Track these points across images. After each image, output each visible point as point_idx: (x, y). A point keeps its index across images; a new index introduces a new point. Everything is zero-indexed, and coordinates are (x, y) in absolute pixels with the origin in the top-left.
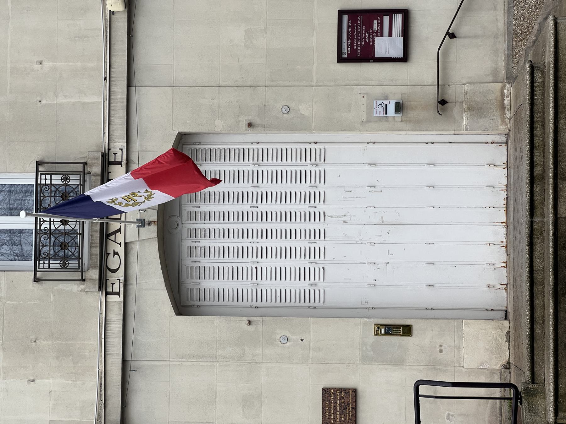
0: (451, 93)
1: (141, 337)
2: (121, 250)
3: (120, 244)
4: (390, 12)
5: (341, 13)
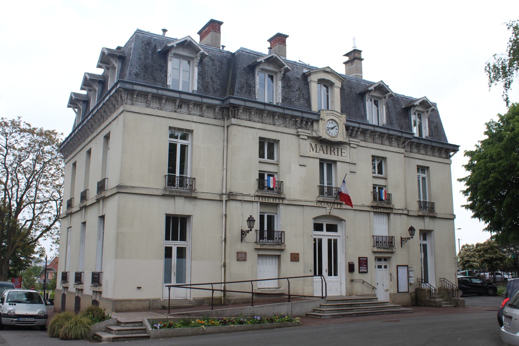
1: (306, 209)
2: (325, 206)
4: (367, 269)
5: (367, 258)
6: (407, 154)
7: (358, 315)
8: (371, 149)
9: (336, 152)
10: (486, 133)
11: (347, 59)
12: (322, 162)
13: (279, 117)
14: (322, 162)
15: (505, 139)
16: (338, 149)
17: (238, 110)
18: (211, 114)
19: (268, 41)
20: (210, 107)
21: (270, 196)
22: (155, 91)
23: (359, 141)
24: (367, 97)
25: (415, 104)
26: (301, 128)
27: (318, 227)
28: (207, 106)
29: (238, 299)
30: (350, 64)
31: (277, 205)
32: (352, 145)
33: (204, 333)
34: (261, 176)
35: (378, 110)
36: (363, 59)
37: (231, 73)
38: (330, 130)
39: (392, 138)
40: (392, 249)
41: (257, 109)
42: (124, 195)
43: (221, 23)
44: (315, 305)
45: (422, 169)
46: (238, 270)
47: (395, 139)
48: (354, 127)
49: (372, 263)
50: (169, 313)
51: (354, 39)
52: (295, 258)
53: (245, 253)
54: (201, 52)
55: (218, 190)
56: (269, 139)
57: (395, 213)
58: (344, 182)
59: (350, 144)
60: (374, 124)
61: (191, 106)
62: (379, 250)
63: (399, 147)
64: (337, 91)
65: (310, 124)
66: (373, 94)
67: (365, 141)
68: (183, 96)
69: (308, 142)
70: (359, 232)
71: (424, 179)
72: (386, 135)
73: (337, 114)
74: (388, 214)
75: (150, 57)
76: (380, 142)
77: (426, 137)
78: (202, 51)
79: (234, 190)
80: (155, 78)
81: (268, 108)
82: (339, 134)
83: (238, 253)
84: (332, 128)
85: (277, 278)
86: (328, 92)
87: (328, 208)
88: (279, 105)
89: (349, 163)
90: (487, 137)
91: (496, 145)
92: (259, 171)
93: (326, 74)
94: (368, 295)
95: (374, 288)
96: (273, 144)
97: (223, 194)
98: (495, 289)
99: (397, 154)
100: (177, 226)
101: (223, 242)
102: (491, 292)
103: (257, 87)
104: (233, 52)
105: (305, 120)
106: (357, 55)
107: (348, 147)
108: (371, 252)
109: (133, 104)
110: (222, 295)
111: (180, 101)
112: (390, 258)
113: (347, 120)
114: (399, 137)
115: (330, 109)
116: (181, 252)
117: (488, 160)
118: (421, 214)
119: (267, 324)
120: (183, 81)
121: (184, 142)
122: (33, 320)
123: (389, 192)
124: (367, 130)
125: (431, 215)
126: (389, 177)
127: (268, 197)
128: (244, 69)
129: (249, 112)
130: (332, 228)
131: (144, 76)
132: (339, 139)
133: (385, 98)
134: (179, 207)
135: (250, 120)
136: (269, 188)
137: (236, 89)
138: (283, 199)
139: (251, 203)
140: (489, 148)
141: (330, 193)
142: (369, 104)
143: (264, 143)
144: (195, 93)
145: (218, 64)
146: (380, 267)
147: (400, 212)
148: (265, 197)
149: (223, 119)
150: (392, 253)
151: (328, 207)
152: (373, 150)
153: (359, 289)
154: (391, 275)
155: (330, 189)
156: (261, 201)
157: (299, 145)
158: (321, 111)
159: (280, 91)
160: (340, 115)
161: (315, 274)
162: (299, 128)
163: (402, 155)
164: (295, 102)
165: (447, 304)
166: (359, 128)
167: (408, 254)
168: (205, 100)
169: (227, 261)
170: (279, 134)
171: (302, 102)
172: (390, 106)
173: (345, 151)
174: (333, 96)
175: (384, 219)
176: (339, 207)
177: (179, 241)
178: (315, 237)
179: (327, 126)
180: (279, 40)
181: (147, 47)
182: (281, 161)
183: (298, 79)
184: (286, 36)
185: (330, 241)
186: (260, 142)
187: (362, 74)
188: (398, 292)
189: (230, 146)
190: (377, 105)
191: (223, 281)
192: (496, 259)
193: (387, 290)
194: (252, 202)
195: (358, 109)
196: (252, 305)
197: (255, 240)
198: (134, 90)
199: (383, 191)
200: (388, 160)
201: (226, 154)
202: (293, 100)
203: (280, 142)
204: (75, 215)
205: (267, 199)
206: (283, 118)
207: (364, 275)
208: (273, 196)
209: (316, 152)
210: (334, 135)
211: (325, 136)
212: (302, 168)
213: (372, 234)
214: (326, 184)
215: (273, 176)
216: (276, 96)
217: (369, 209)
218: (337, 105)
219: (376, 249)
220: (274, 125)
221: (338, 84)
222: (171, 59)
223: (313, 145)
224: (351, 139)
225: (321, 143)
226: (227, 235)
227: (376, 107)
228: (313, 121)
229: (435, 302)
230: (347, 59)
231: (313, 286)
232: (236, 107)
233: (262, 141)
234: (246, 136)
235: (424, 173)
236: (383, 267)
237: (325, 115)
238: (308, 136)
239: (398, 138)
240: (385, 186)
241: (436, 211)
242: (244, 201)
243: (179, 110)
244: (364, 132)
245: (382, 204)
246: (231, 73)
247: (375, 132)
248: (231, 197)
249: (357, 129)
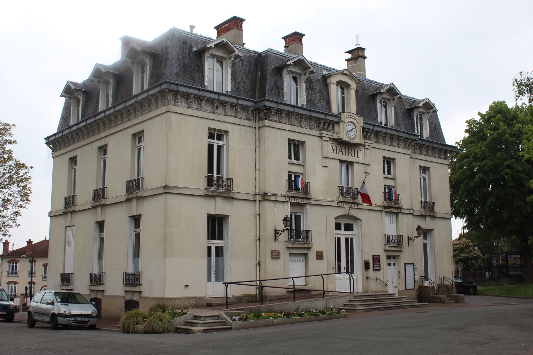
0: (369, 280)
1: (329, 209)
4: (380, 266)
6: (412, 155)
7: (385, 309)
8: (383, 151)
10: (466, 131)
11: (349, 56)
15: (488, 140)
17: (271, 112)
18: (242, 114)
19: (283, 38)
20: (245, 108)
22: (196, 92)
25: (419, 105)
27: (338, 227)
28: (242, 107)
29: (273, 296)
30: (353, 61)
31: (303, 205)
32: (367, 147)
33: (273, 325)
36: (366, 58)
37: (259, 74)
40: (401, 248)
42: (171, 195)
43: (242, 20)
44: (345, 300)
45: (424, 169)
46: (273, 268)
48: (369, 129)
49: (384, 261)
50: (227, 308)
51: (357, 36)
52: (320, 256)
53: (279, 252)
54: (236, 53)
55: (251, 190)
57: (402, 213)
58: (364, 183)
61: (204, 102)
62: (390, 248)
64: (353, 93)
65: (331, 126)
66: (384, 96)
68: (222, 98)
70: (373, 231)
71: (424, 179)
72: (396, 137)
74: (397, 214)
75: (188, 57)
76: (389, 143)
77: (427, 138)
78: (237, 52)
79: (268, 190)
80: (193, 79)
81: (297, 111)
83: (272, 251)
84: (351, 131)
85: (304, 275)
87: (347, 208)
88: (304, 107)
90: (467, 135)
91: (480, 144)
93: (344, 76)
94: (381, 292)
95: (386, 285)
96: (298, 145)
97: (256, 194)
98: (475, 288)
99: (405, 155)
100: (216, 225)
101: (258, 241)
102: (471, 291)
103: (285, 89)
104: (260, 52)
105: (327, 122)
106: (360, 53)
107: (363, 148)
108: (383, 251)
109: (175, 105)
110: (258, 292)
111: (217, 102)
112: (398, 256)
113: (363, 123)
114: (406, 138)
116: (220, 251)
117: (471, 159)
118: (423, 213)
119: (321, 316)
120: (217, 81)
121: (220, 143)
122: (87, 319)
123: (398, 193)
124: (380, 132)
125: (432, 214)
127: (297, 197)
128: (273, 71)
130: (349, 227)
131: (184, 76)
132: (357, 141)
134: (220, 207)
137: (267, 91)
138: (309, 199)
140: (472, 147)
144: (229, 94)
145: (245, 63)
146: (389, 265)
147: (407, 212)
149: (255, 120)
150: (401, 251)
151: (347, 207)
152: (385, 151)
153: (374, 287)
154: (399, 272)
157: (322, 147)
159: (304, 93)
161: (339, 271)
162: (322, 130)
163: (408, 156)
164: (317, 104)
165: (447, 300)
166: (373, 130)
167: (412, 253)
168: (240, 102)
169: (261, 260)
174: (349, 98)
175: (393, 218)
177: (217, 241)
178: (347, 236)
179: (347, 128)
180: (294, 39)
181: (184, 46)
183: (319, 80)
184: (303, 35)
185: (347, 239)
186: (289, 143)
187: (365, 72)
188: (406, 289)
189: (262, 147)
191: (258, 279)
192: (472, 259)
193: (395, 287)
194: (283, 202)
195: (370, 110)
196: (294, 301)
197: (286, 239)
198: (179, 91)
201: (258, 155)
202: (315, 102)
203: (306, 144)
204: (79, 213)
205: (296, 199)
207: (377, 272)
210: (352, 137)
211: (346, 139)
212: (325, 169)
213: (384, 234)
216: (301, 98)
217: (381, 209)
218: (352, 106)
219: (387, 248)
221: (354, 86)
222: (207, 60)
223: (334, 147)
224: (366, 141)
226: (261, 234)
229: (439, 298)
230: (349, 56)
231: (335, 282)
232: (269, 109)
234: (277, 137)
235: (425, 174)
236: (392, 265)
238: (330, 138)
240: (394, 187)
241: (436, 211)
242: (277, 201)
243: (216, 111)
244: (377, 134)
245: (392, 204)
246: (259, 74)
247: (387, 134)
248: (265, 197)
249: (373, 132)
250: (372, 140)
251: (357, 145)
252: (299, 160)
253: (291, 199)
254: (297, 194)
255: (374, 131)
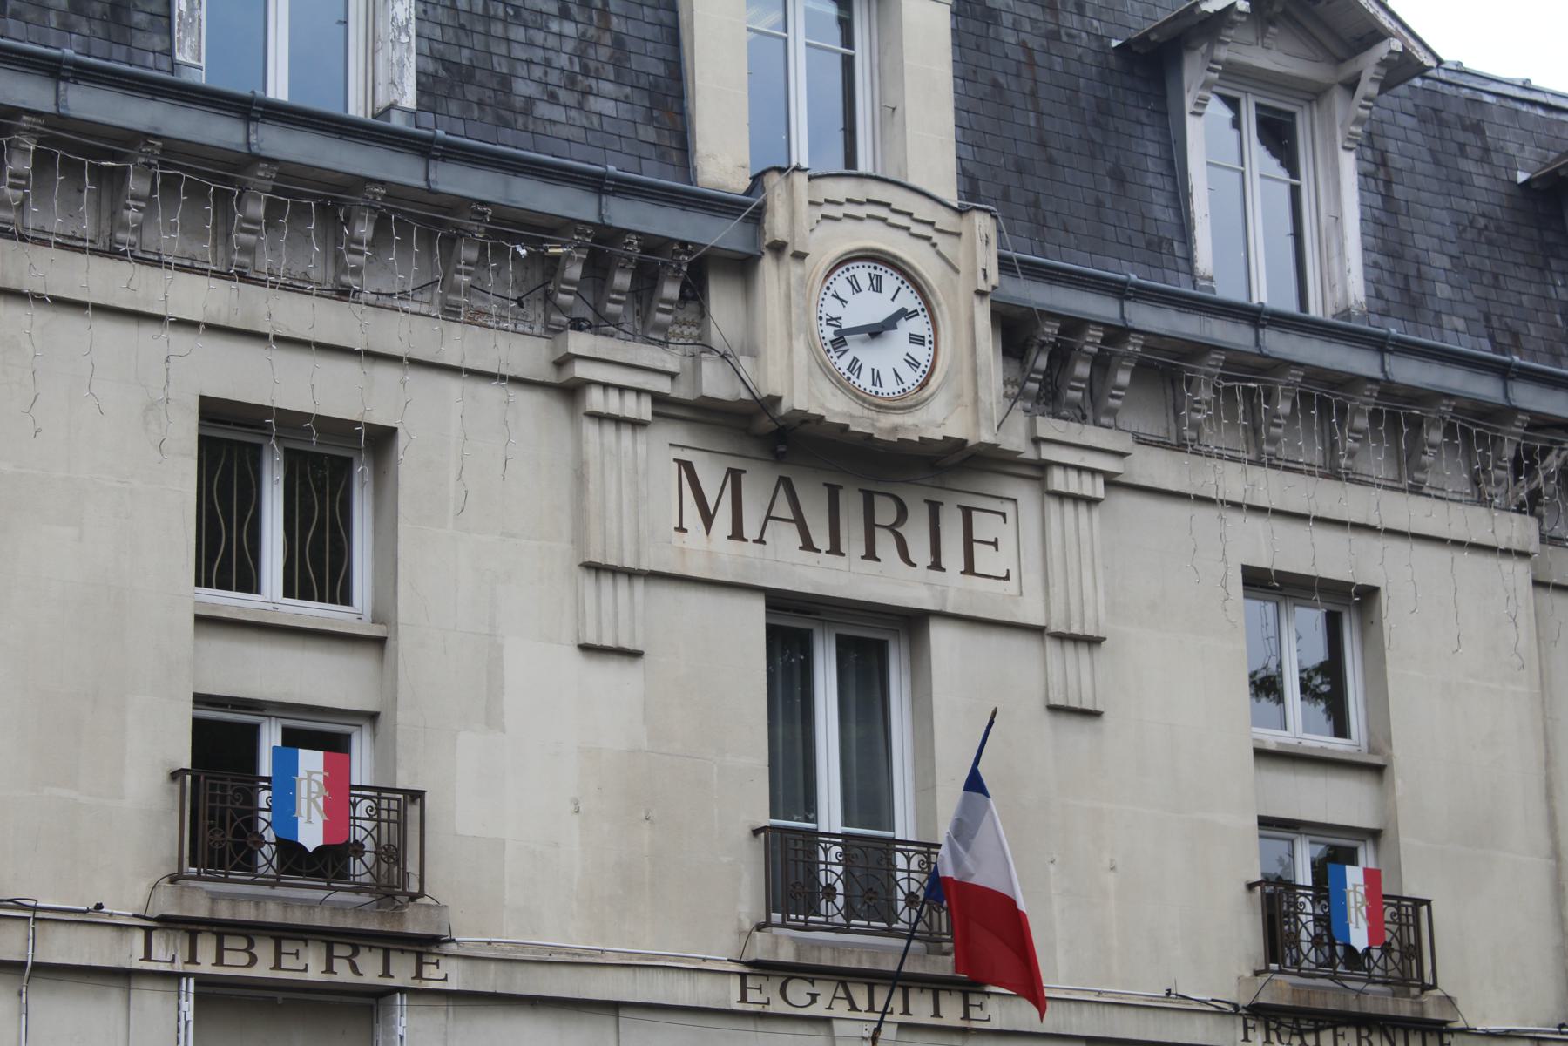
2: (818, 1010)
3: (830, 1008)
8: (1236, 519)
9: (917, 536)
12: (792, 623)
13: (381, 225)
14: (792, 623)
16: (934, 509)
21: (297, 917)
23: (1121, 442)
24: (1194, 74)
26: (599, 324)
31: (370, 1004)
32: (1058, 480)
34: (223, 746)
35: (1295, 192)
38: (857, 349)
39: (1416, 424)
41: (174, 151)
47: (1450, 431)
48: (1073, 325)
56: (291, 421)
58: (974, 783)
59: (1042, 468)
60: (1261, 296)
63: (1482, 501)
65: (671, 290)
67: (1181, 446)
69: (657, 454)
72: (1366, 400)
73: (923, 209)
76: (1314, 454)
82: (952, 387)
84: (875, 332)
86: (848, 40)
88: (397, 121)
89: (1037, 631)
92: (200, 700)
96: (341, 471)
99: (1464, 557)
107: (1024, 493)
113: (1005, 265)
115: (864, 165)
123: (1412, 889)
124: (1197, 350)
126: (1402, 758)
127: (281, 934)
129: (98, 174)
132: (940, 420)
133: (1351, 86)
135: (113, 252)
136: (293, 857)
138: (426, 946)
139: (115, 994)
141: (870, 892)
142: (1211, 136)
143: (254, 455)
148: (250, 931)
155: (870, 859)
156: (206, 965)
157: (580, 476)
158: (773, 180)
160: (945, 219)
162: (577, 325)
163: (1520, 573)
164: (544, 110)
166: (1117, 333)
170: (386, 374)
171: (608, 107)
172: (1396, 161)
173: (1006, 534)
176: (952, 1013)
179: (832, 308)
182: (403, 615)
186: (206, 445)
190: (1290, 163)
194: (123, 976)
195: (1119, 178)
199: (1354, 876)
200: (1391, 610)
202: (522, 88)
203: (404, 443)
206: (427, 238)
208: (321, 919)
209: (737, 534)
210: (890, 387)
214: (830, 816)
215: (335, 745)
220: (344, 294)
223: (711, 478)
224: (1048, 427)
225: (778, 458)
227: (1282, 174)
228: (700, 272)
233: (230, 442)
237: (806, 215)
238: (658, 399)
239: (1475, 426)
240: (1374, 835)
244: (1166, 368)
250: (1126, 419)
251: (951, 467)
252: (346, 599)
253: (264, 951)
254: (309, 902)
255: (1134, 345)
